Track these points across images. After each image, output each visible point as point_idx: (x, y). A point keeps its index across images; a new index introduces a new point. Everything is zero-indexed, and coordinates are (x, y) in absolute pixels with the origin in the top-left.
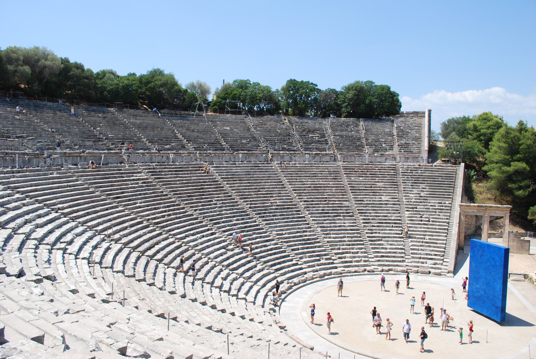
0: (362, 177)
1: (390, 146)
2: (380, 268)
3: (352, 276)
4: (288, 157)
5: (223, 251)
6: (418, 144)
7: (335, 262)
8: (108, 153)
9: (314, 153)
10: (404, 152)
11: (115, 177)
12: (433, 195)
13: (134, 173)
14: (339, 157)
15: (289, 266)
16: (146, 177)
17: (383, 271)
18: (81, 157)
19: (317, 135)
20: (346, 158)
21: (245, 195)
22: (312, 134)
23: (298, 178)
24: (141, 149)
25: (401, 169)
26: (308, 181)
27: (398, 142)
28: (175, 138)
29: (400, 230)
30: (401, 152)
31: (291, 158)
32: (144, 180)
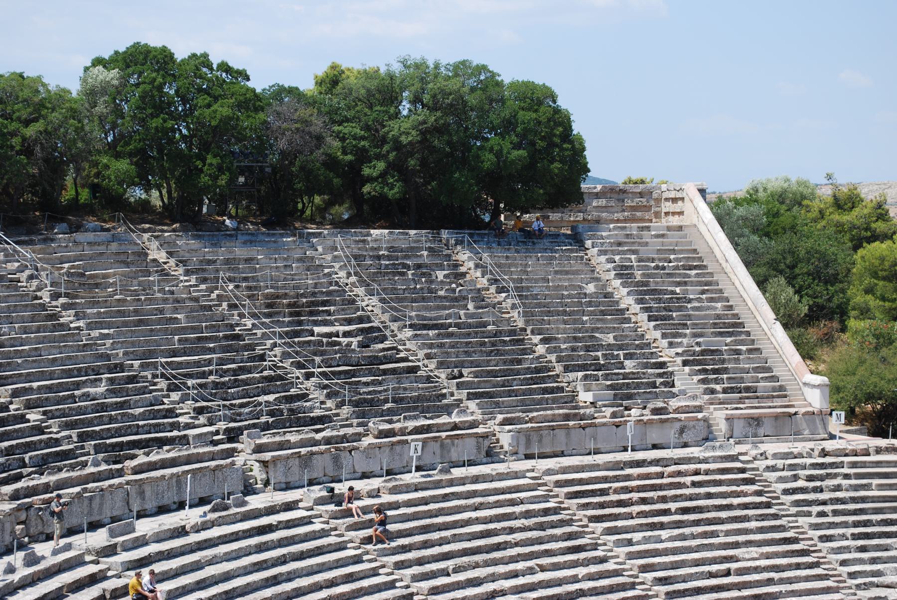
0: (662, 526)
4: (327, 456)
6: (750, 351)
9: (411, 424)
10: (725, 391)
14: (505, 439)
19: (342, 329)
20: (535, 437)
22: (316, 323)
23: (450, 564)
25: (772, 476)
26: (493, 578)
27: (671, 345)
30: (713, 391)
31: (336, 460)
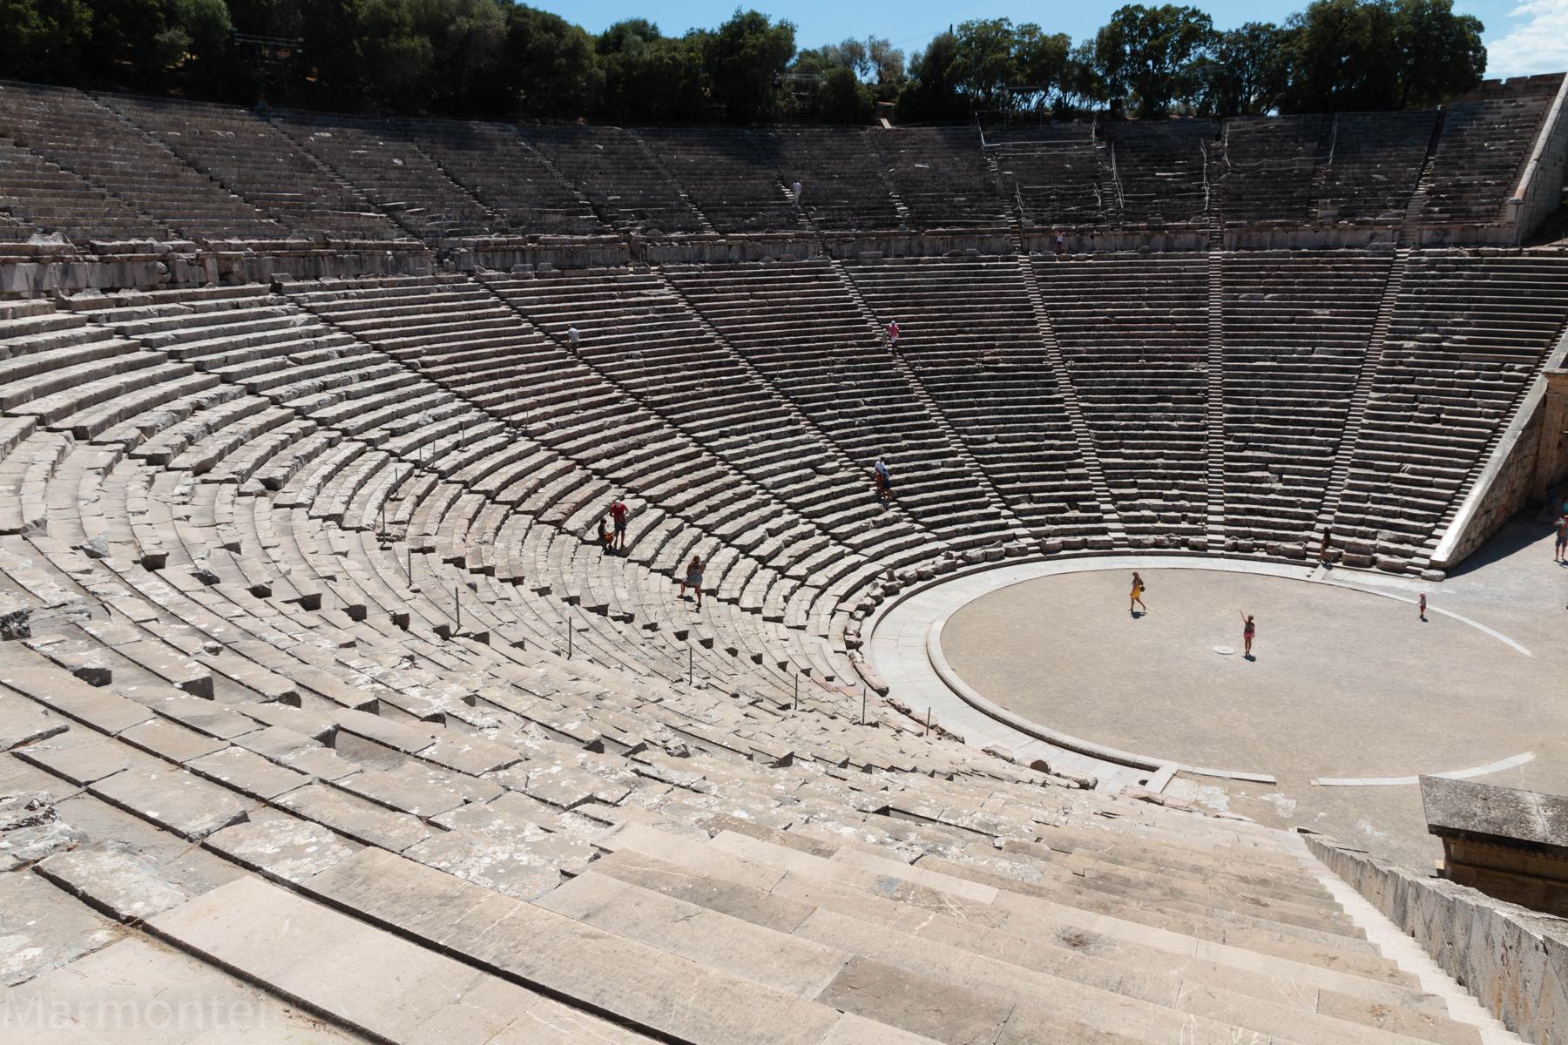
0: (1275, 291)
1: (1403, 195)
2: (1229, 541)
3: (1143, 554)
5: (809, 471)
7: (1106, 517)
8: (592, 242)
11: (594, 298)
12: (1477, 345)
13: (645, 287)
15: (971, 519)
16: (672, 297)
17: (1235, 547)
18: (522, 251)
21: (919, 342)
24: (680, 229)
28: (776, 199)
29: (1330, 444)
32: (663, 307)
